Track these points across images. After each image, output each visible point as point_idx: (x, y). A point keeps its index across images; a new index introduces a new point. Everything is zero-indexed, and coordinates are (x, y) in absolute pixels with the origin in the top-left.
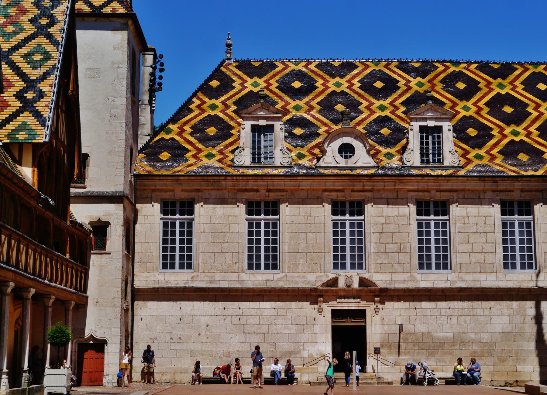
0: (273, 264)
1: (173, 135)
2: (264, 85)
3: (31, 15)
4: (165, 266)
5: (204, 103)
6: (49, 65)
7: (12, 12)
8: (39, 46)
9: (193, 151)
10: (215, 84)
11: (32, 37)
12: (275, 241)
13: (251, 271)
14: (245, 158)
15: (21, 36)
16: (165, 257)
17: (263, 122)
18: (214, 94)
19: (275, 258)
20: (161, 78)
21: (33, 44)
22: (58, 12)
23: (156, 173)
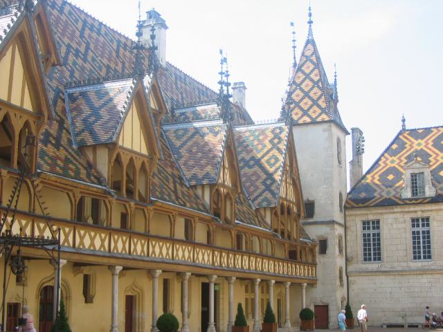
0: (428, 256)
1: (368, 181)
2: (424, 144)
4: (365, 260)
5: (387, 159)
6: (277, 165)
7: (261, 137)
9: (379, 190)
10: (395, 146)
11: (271, 149)
12: (429, 242)
13: (415, 260)
14: (407, 194)
15: (265, 150)
16: (365, 254)
17: (417, 171)
18: (394, 153)
19: (429, 252)
20: (363, 145)
21: (270, 154)
23: (355, 205)
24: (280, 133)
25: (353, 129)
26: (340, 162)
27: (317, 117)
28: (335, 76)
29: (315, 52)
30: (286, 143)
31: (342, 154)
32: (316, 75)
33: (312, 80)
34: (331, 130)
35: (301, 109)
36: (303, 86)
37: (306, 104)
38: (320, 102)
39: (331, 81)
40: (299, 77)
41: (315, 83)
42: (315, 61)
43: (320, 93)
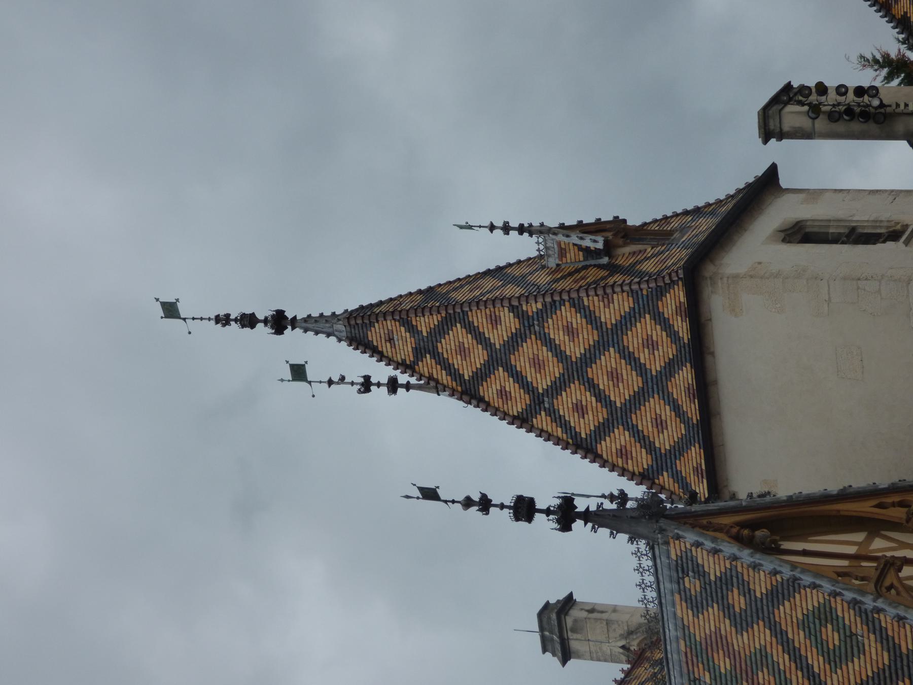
3: (726, 626)
7: (724, 664)
8: (804, 624)
15: (783, 660)
20: (841, 90)
21: (799, 638)
22: (714, 568)
24: (700, 572)
25: (767, 134)
26: (894, 235)
27: (673, 336)
28: (506, 228)
29: (398, 310)
30: (746, 555)
31: (863, 215)
32: (495, 321)
33: (515, 341)
34: (736, 277)
35: (638, 400)
36: (542, 383)
37: (615, 376)
38: (609, 315)
39: (526, 248)
40: (503, 394)
41: (529, 327)
42: (435, 320)
43: (567, 313)
